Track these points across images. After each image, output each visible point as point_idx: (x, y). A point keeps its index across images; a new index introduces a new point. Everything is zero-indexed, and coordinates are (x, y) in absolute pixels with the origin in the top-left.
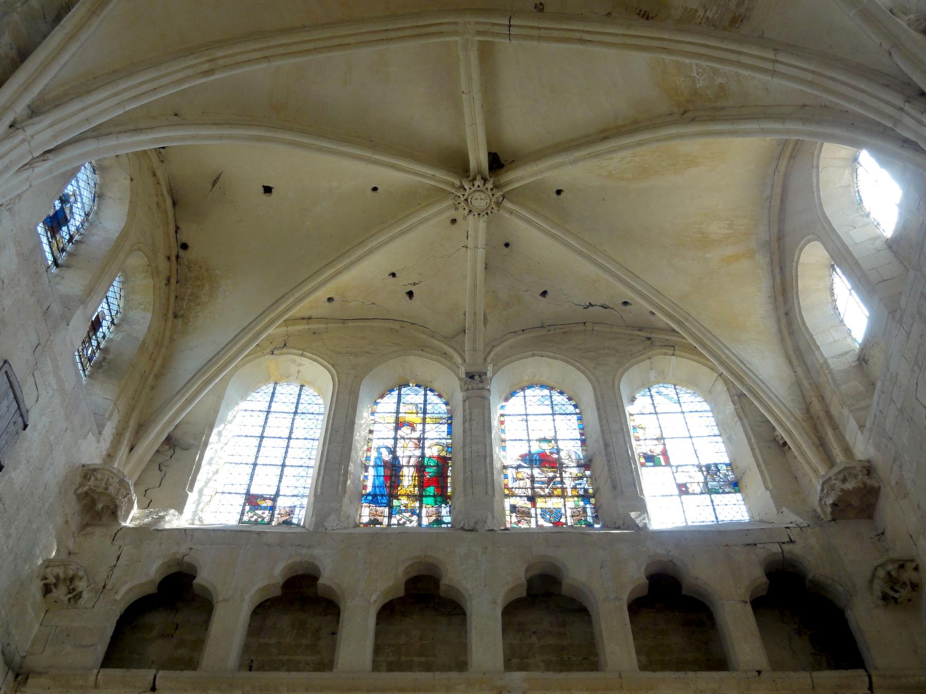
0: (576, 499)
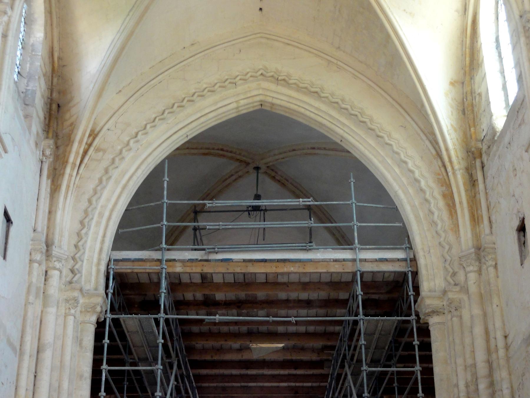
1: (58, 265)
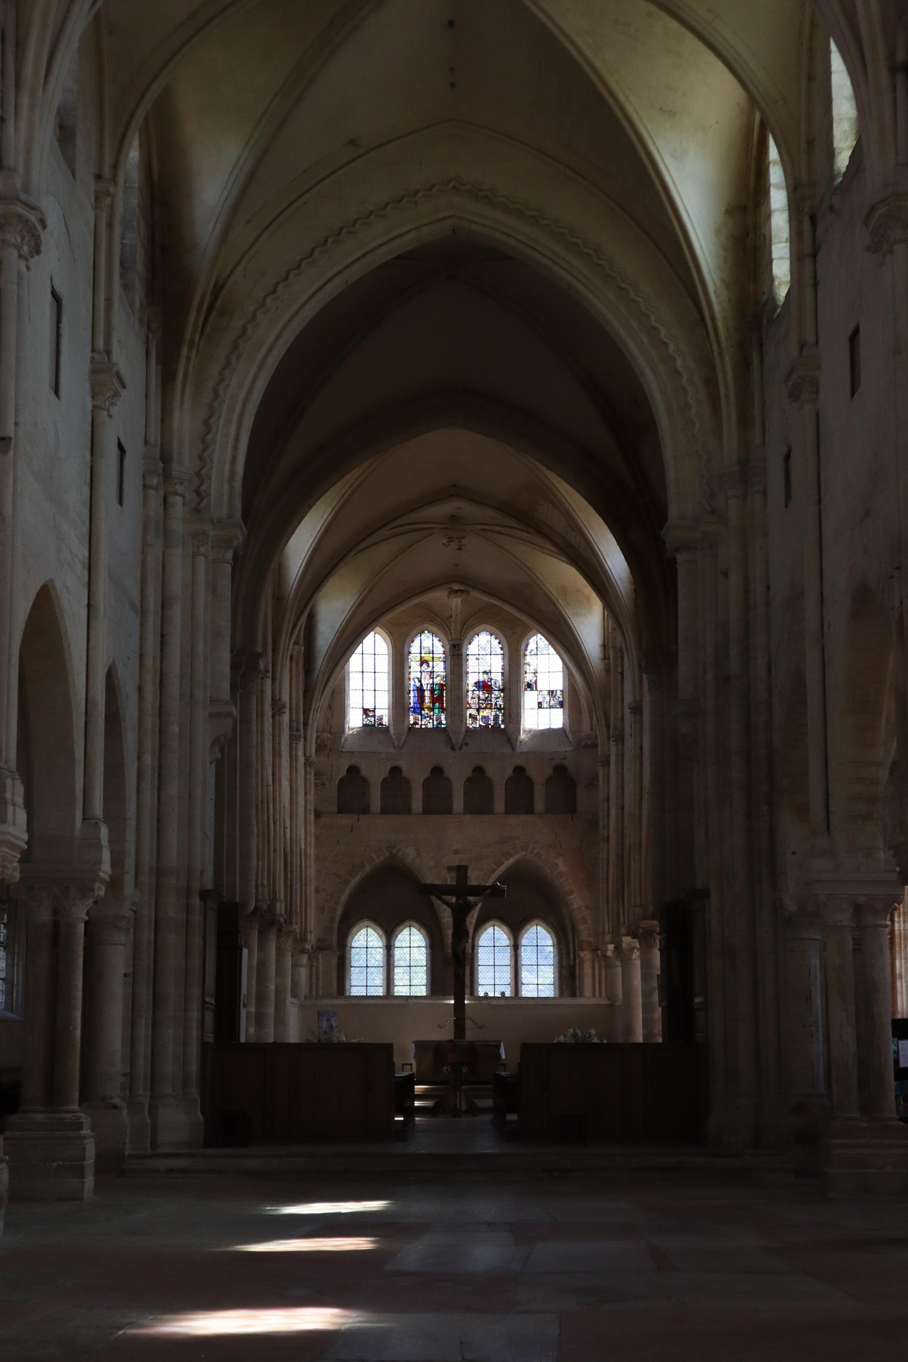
0: (496, 710)
1: (179, 489)
